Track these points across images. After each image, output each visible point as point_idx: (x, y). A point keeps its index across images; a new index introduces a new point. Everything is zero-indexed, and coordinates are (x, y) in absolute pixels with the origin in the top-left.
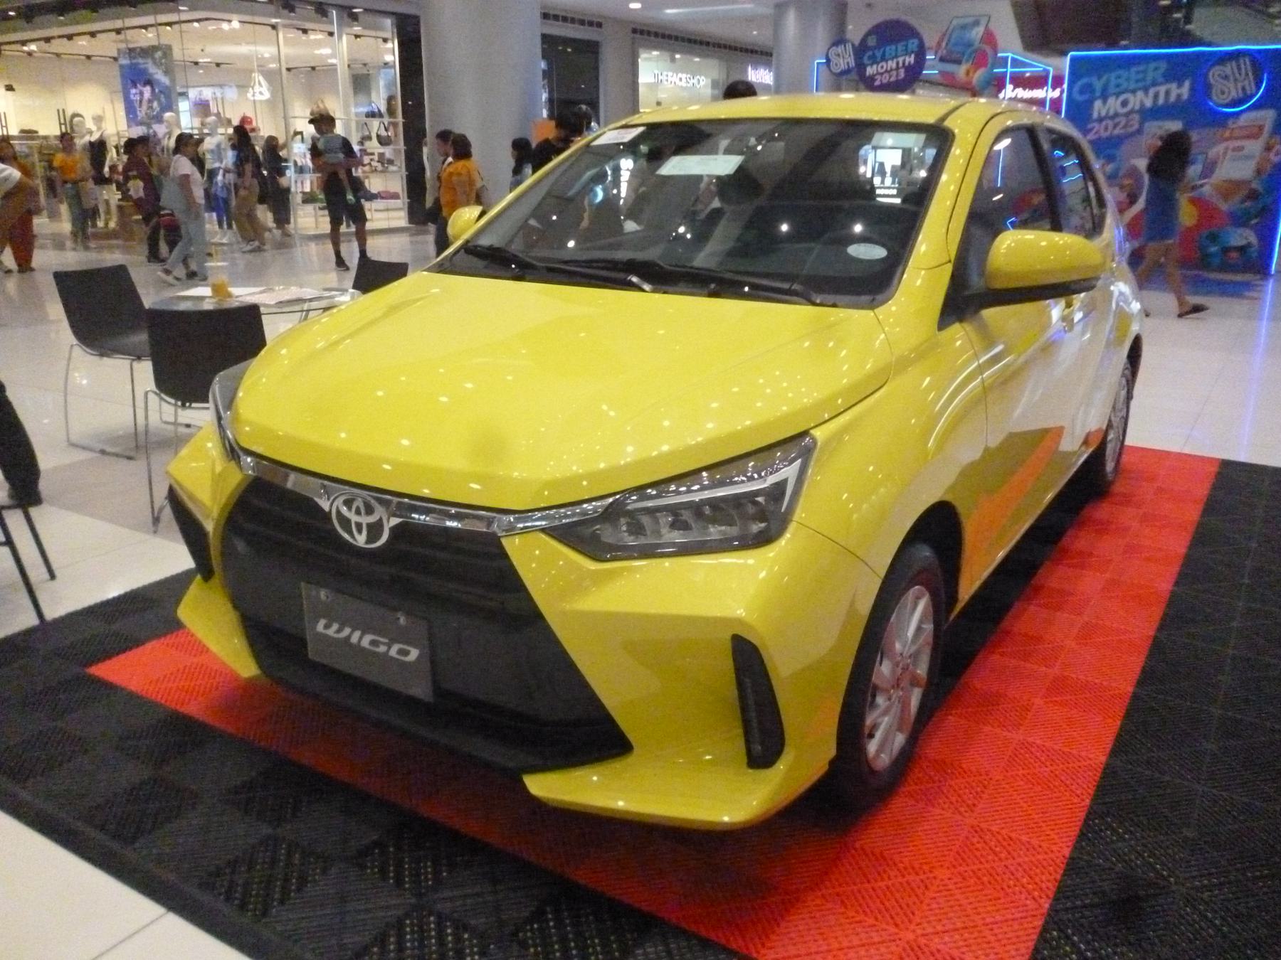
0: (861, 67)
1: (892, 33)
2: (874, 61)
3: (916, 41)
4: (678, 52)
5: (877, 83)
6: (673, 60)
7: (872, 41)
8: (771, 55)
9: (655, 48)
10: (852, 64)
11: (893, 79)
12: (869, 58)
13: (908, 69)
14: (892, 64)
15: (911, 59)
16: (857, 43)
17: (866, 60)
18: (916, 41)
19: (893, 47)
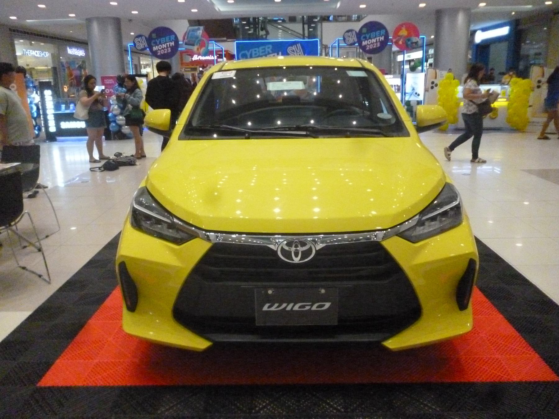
2: (156, 44)
4: (33, 40)
5: (159, 54)
6: (31, 44)
7: (154, 36)
8: (87, 44)
9: (22, 39)
10: (146, 46)
11: (166, 52)
16: (147, 36)
17: (153, 45)
18: (174, 36)
19: (164, 38)
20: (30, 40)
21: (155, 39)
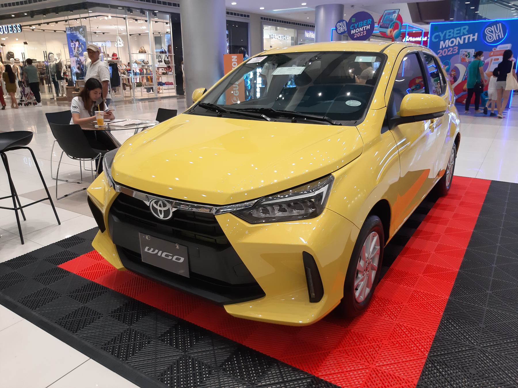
0: (349, 31)
1: (362, 17)
3: (371, 20)
5: (355, 37)
6: (276, 29)
7: (354, 20)
10: (346, 30)
12: (352, 27)
13: (367, 31)
14: (361, 29)
15: (368, 27)
17: (351, 28)
18: (371, 20)
19: (362, 22)
20: (277, 26)
21: (354, 23)
